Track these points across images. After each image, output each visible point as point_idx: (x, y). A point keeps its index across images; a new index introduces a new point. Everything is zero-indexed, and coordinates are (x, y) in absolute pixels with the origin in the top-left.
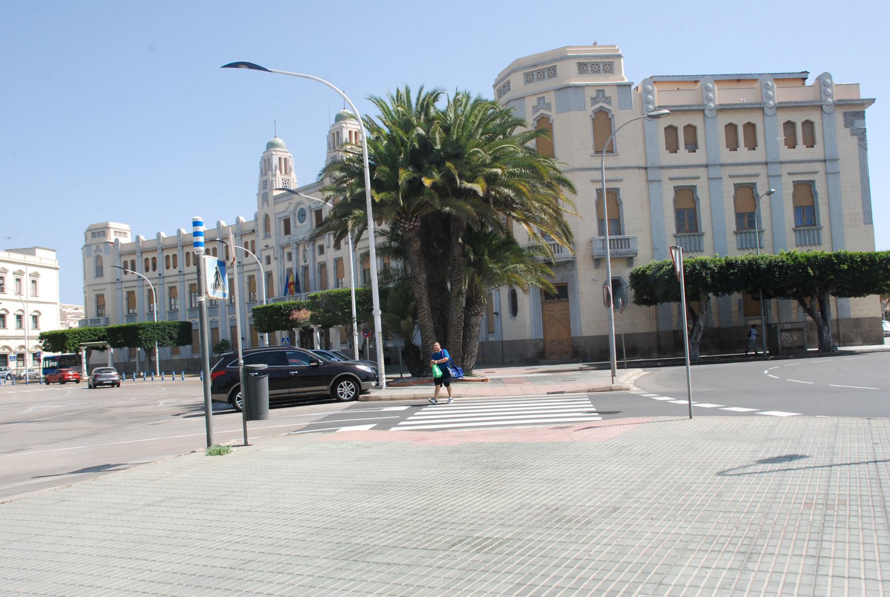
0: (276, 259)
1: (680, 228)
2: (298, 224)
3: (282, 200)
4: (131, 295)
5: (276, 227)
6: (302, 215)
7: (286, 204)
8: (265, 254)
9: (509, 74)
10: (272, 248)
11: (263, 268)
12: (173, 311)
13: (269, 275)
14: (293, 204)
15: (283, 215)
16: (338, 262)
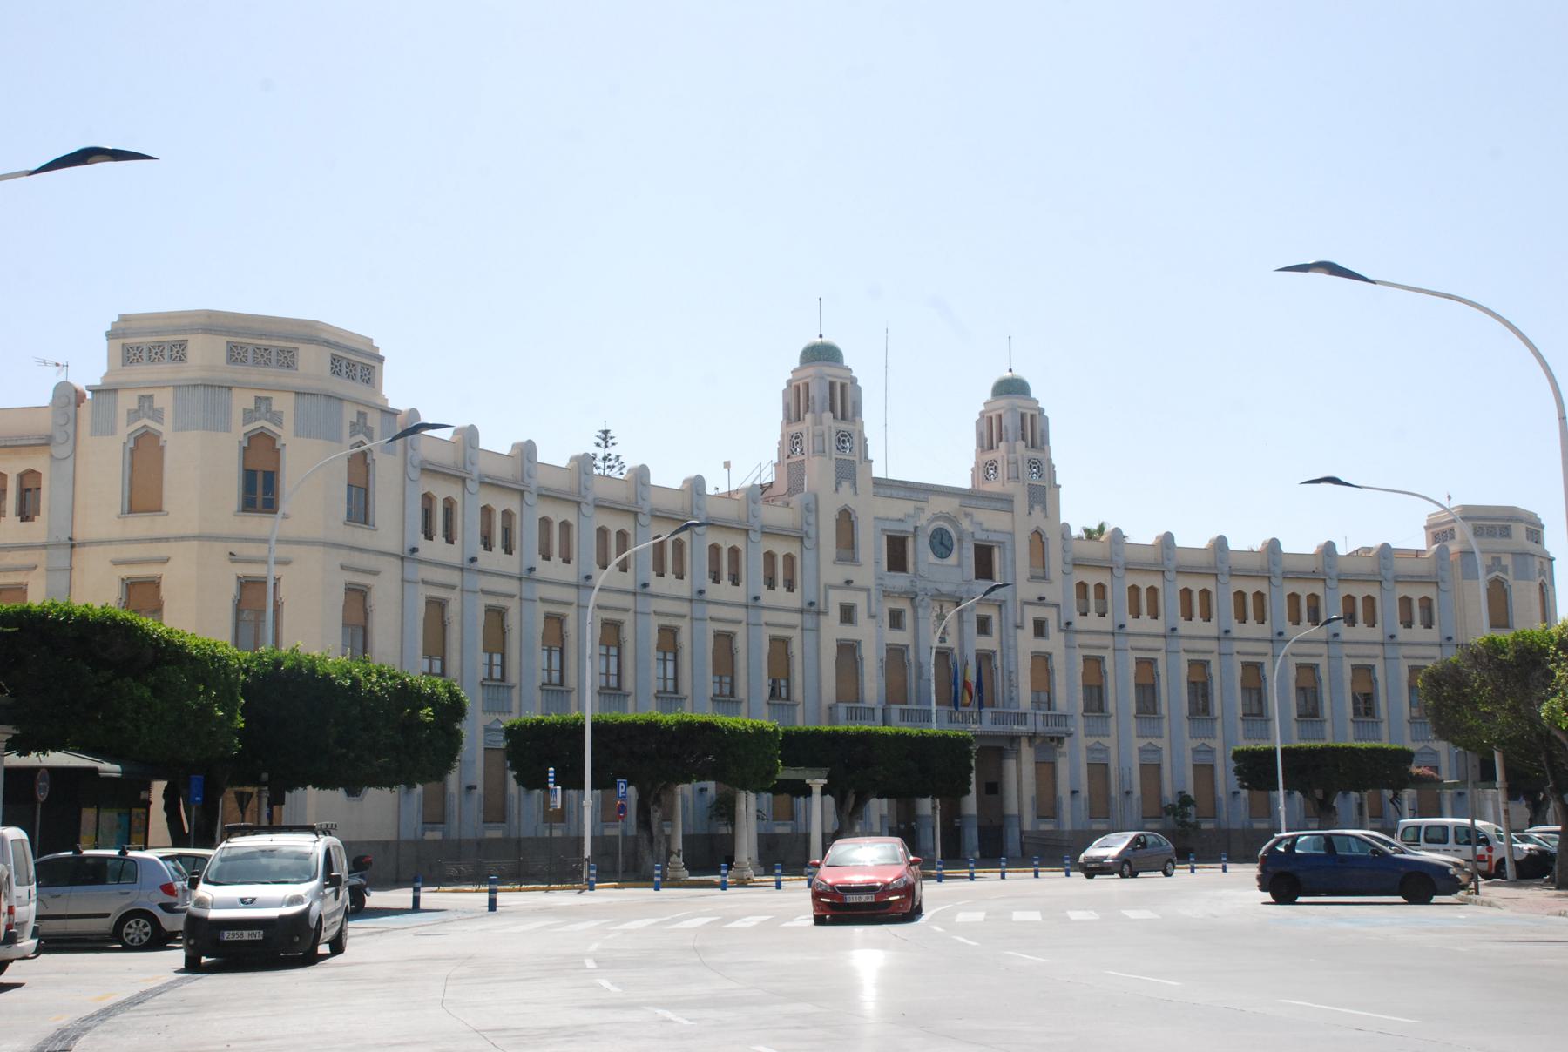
0: (872, 616)
1: (1356, 712)
2: (932, 558)
3: (895, 493)
4: (437, 607)
5: (872, 547)
6: (942, 543)
7: (908, 507)
8: (837, 598)
9: (1510, 519)
10: (868, 590)
11: (833, 630)
12: (670, 695)
13: (848, 652)
14: (928, 514)
15: (902, 527)
16: (1042, 662)
